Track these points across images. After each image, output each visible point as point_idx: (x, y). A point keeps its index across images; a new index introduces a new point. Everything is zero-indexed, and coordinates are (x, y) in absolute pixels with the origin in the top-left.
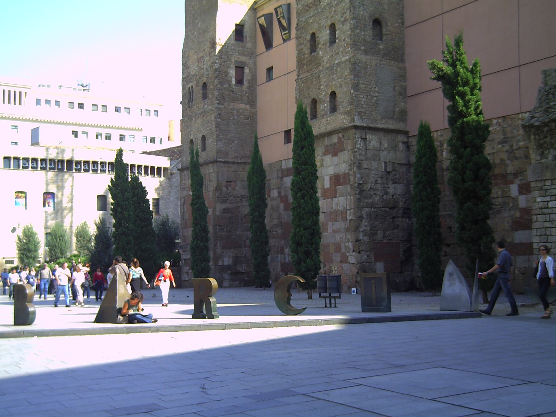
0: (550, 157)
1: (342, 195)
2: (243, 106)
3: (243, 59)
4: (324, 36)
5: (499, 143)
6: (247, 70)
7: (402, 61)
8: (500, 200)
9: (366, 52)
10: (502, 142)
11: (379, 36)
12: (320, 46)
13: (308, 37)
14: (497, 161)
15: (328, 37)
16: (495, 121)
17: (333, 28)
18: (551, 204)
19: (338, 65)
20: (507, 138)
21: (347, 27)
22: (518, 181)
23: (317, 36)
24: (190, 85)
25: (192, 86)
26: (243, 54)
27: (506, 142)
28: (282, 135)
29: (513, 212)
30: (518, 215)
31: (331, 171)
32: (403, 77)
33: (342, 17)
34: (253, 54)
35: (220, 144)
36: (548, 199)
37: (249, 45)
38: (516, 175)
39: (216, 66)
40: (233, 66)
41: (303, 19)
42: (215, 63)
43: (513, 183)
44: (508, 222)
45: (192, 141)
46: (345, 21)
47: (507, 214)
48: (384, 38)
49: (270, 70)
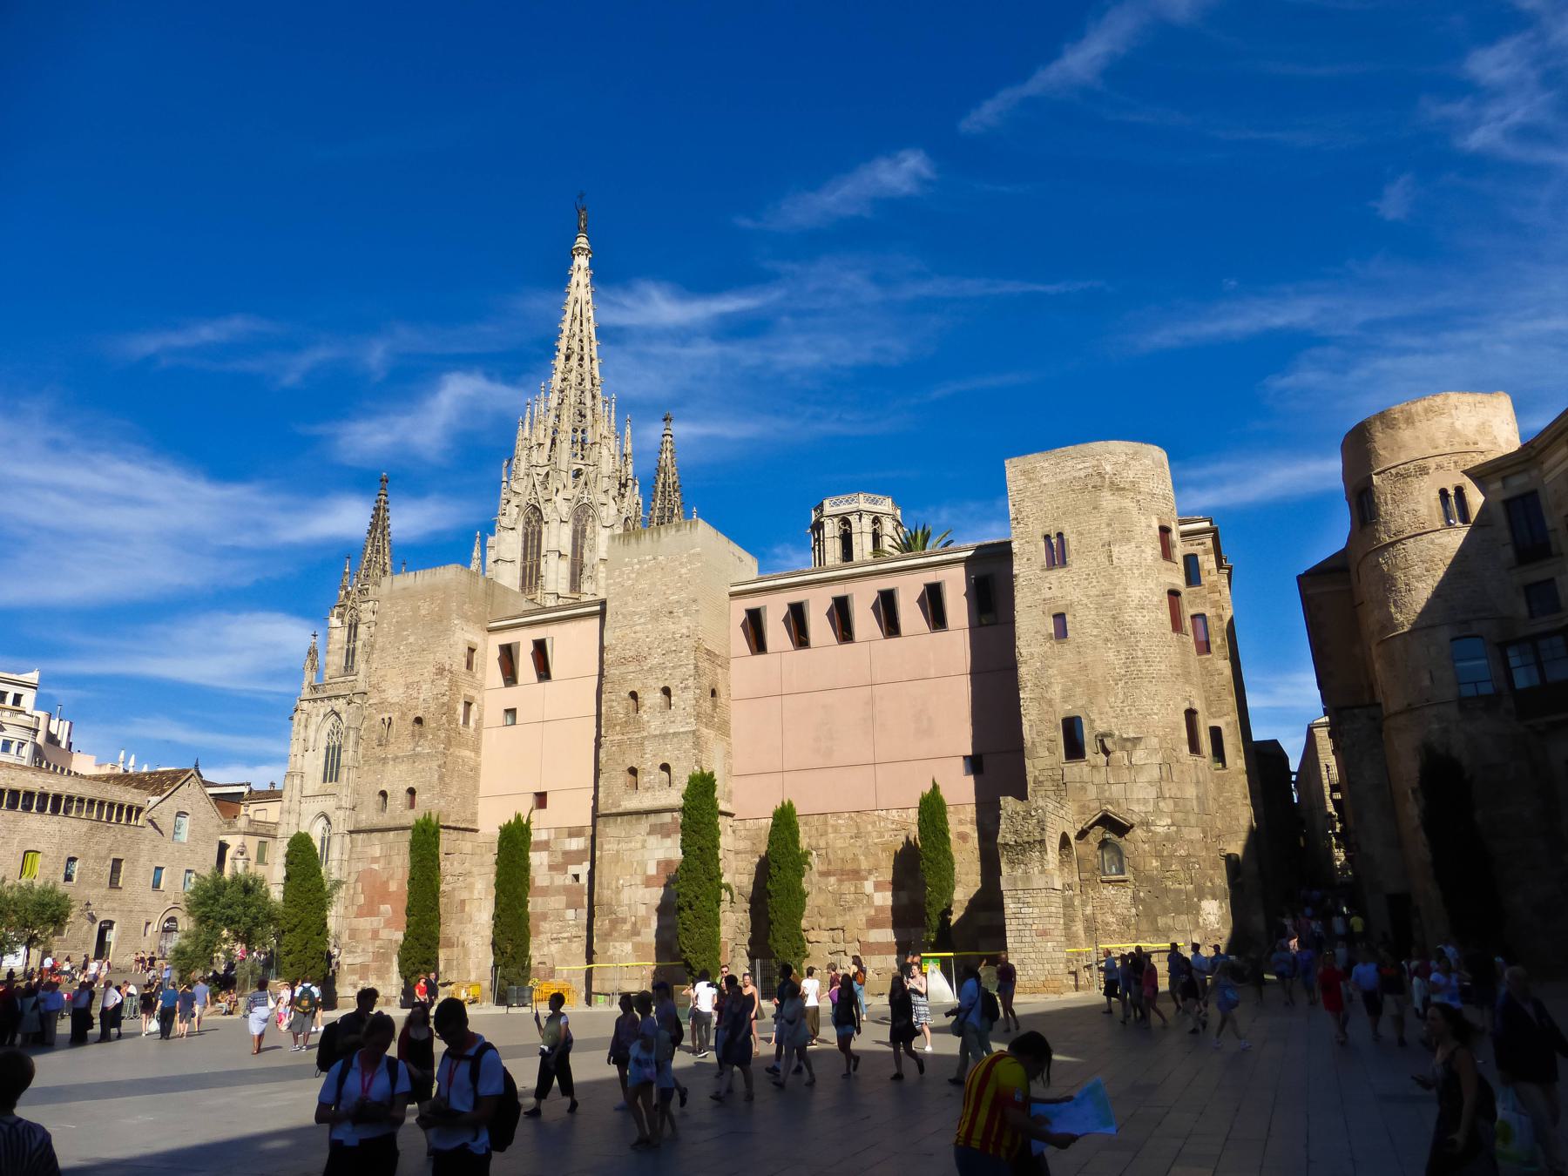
2: (467, 753)
3: (472, 692)
4: (652, 698)
6: (474, 707)
7: (728, 736)
9: (707, 725)
11: (715, 706)
14: (850, 856)
17: (666, 691)
21: (690, 695)
22: (872, 879)
24: (386, 716)
26: (471, 686)
28: (530, 801)
30: (873, 912)
31: (661, 855)
32: (728, 754)
34: (480, 687)
35: (442, 803)
37: (479, 676)
38: (870, 872)
39: (446, 699)
45: (383, 794)
49: (511, 712)
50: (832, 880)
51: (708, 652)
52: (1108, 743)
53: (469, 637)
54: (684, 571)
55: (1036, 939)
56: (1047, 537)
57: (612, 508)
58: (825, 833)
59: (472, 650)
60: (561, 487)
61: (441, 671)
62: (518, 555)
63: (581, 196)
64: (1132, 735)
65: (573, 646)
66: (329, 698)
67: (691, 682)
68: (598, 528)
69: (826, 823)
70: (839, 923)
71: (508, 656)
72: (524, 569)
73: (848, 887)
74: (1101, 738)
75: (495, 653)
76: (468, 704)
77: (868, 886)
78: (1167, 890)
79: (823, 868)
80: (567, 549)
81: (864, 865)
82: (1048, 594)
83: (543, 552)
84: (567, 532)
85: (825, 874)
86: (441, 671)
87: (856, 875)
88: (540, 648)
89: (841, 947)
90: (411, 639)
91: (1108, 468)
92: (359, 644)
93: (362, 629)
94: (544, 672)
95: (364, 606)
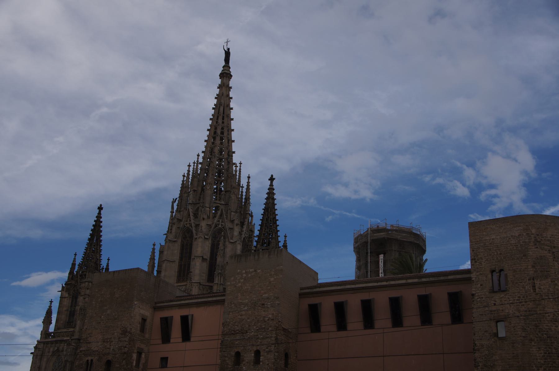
3: (143, 346)
11: (286, 364)
12: (244, 363)
13: (233, 354)
15: (253, 358)
17: (258, 353)
23: (241, 354)
24: (90, 358)
25: (92, 360)
33: (267, 348)
37: (147, 336)
39: (126, 349)
40: (135, 351)
41: (229, 339)
42: (125, 347)
46: (270, 351)
48: (289, 366)
49: (164, 361)
51: (284, 329)
53: (142, 312)
54: (272, 279)
56: (493, 271)
57: (237, 230)
59: (144, 320)
60: (205, 217)
61: (124, 332)
62: (177, 257)
63: (227, 42)
65: (206, 320)
66: (56, 342)
67: (273, 348)
68: (227, 243)
71: (166, 323)
72: (180, 266)
75: (157, 321)
76: (139, 354)
80: (207, 256)
82: (494, 308)
83: (192, 258)
84: (208, 244)
86: (124, 332)
88: (185, 321)
90: (109, 312)
91: (534, 231)
92: (78, 308)
93: (80, 299)
94: (186, 336)
95: (83, 285)
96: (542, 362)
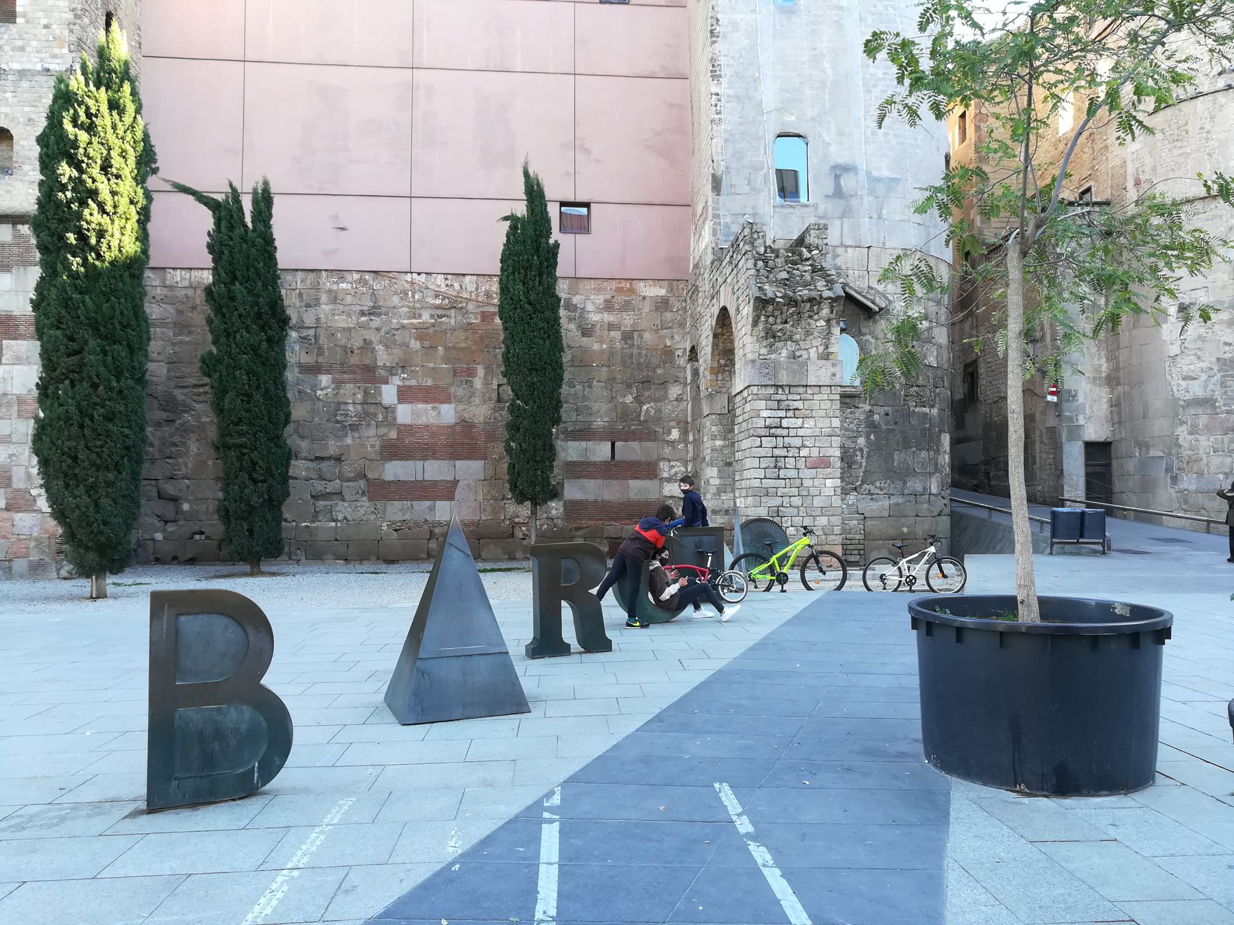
0: (784, 353)
1: (18, 361)
5: (363, 313)
8: (359, 408)
10: (373, 312)
14: (357, 343)
16: (356, 276)
18: (785, 423)
19: (22, 73)
20: (379, 307)
22: (396, 381)
27: (379, 315)
29: (383, 430)
30: (393, 434)
36: (782, 414)
38: (391, 371)
43: (387, 383)
44: (373, 446)
47: (372, 432)
50: (325, 379)
52: (847, 182)
55: (807, 473)
58: (317, 302)
64: (886, 173)
69: (316, 287)
70: (332, 447)
73: (352, 394)
74: (839, 171)
77: (389, 394)
78: (910, 414)
79: (306, 359)
81: (383, 357)
85: (313, 370)
87: (370, 375)
89: (335, 485)
96: (880, 75)
